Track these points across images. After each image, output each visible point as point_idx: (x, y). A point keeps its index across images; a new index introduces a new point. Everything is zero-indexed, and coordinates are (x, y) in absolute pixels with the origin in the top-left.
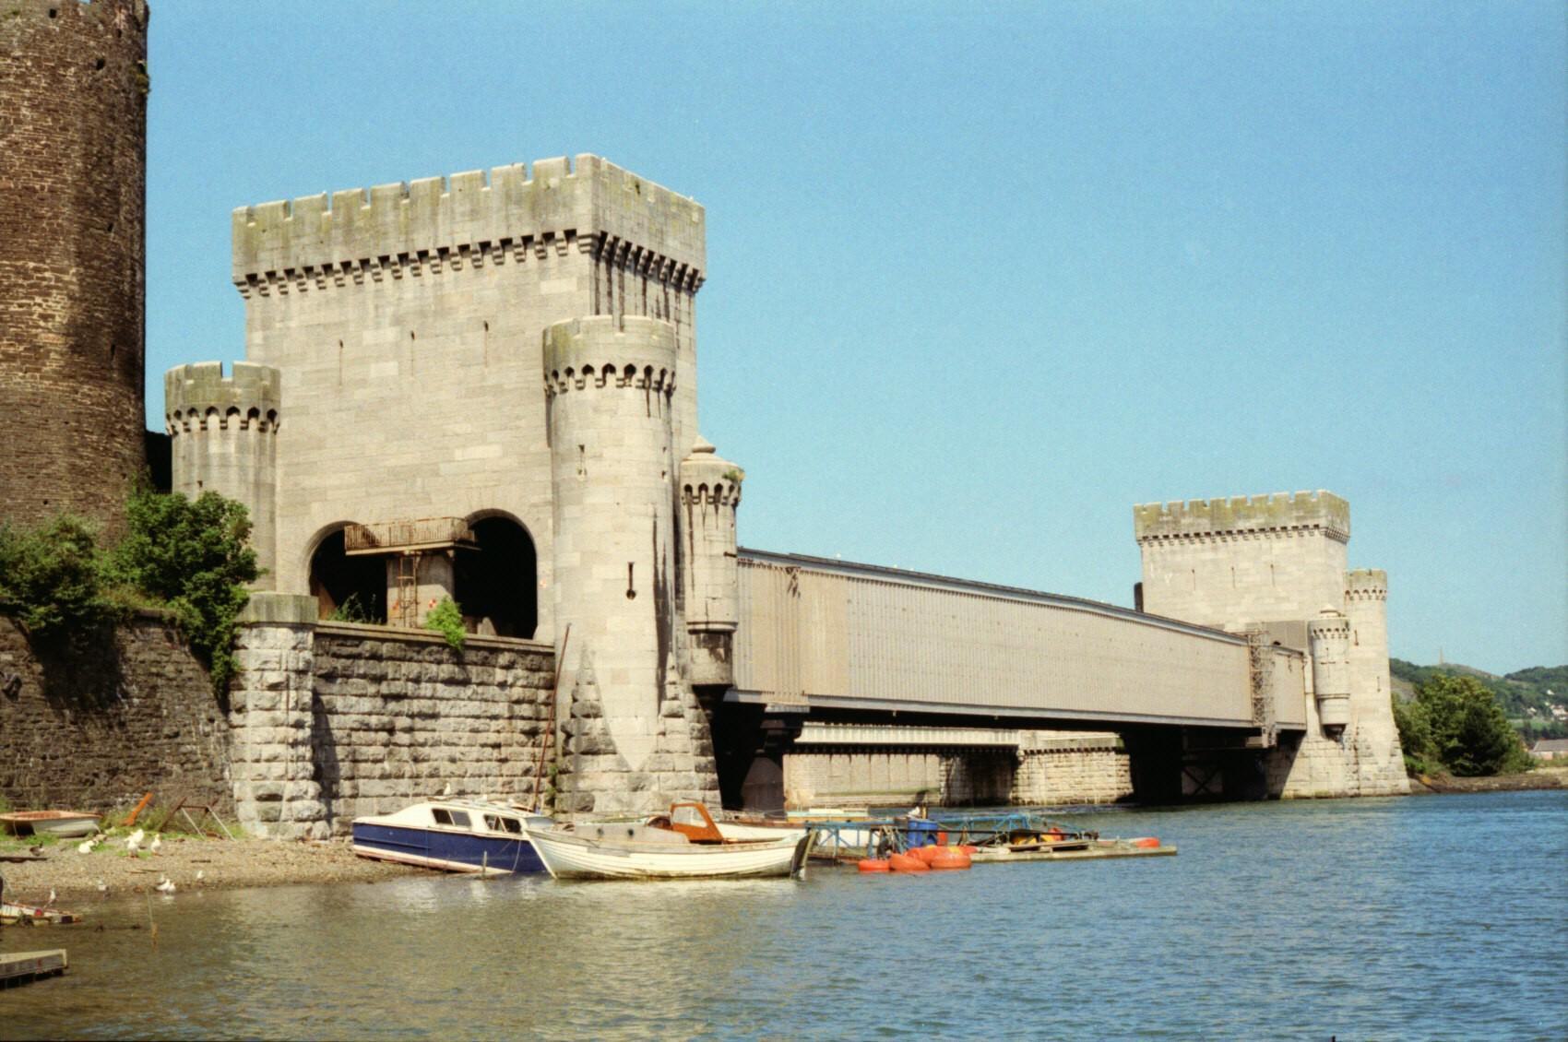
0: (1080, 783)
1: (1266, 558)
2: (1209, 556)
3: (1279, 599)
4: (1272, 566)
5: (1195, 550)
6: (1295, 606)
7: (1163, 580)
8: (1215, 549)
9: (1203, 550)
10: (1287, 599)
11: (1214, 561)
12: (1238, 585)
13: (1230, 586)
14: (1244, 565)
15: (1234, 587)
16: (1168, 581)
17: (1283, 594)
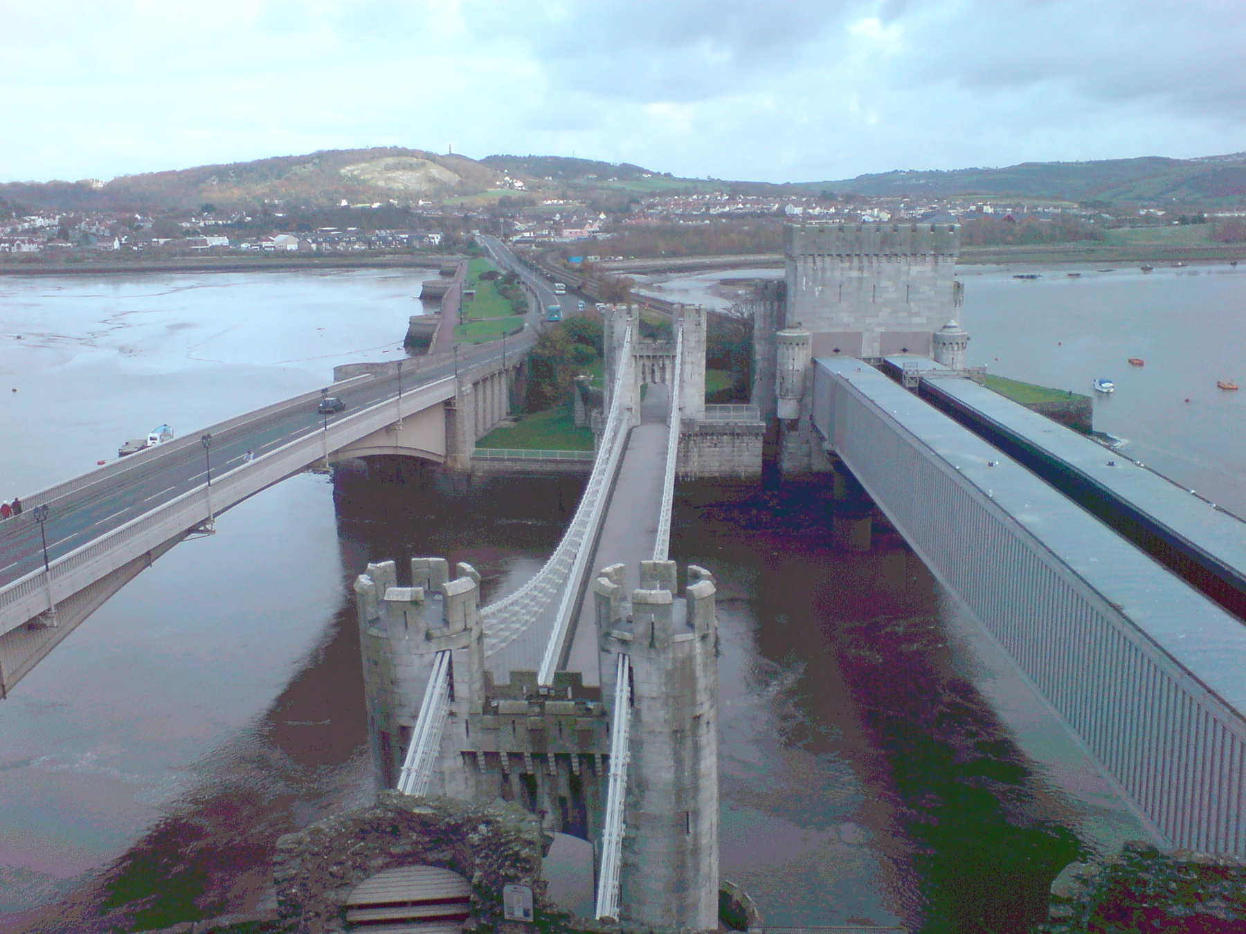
0: (729, 461)
1: (903, 279)
2: (855, 274)
3: (912, 314)
4: (908, 286)
5: (842, 269)
6: (924, 320)
7: (814, 292)
8: (861, 269)
9: (851, 269)
10: (917, 314)
11: (860, 279)
12: (876, 300)
13: (872, 300)
14: (885, 283)
15: (874, 300)
16: (817, 293)
17: (915, 310)
